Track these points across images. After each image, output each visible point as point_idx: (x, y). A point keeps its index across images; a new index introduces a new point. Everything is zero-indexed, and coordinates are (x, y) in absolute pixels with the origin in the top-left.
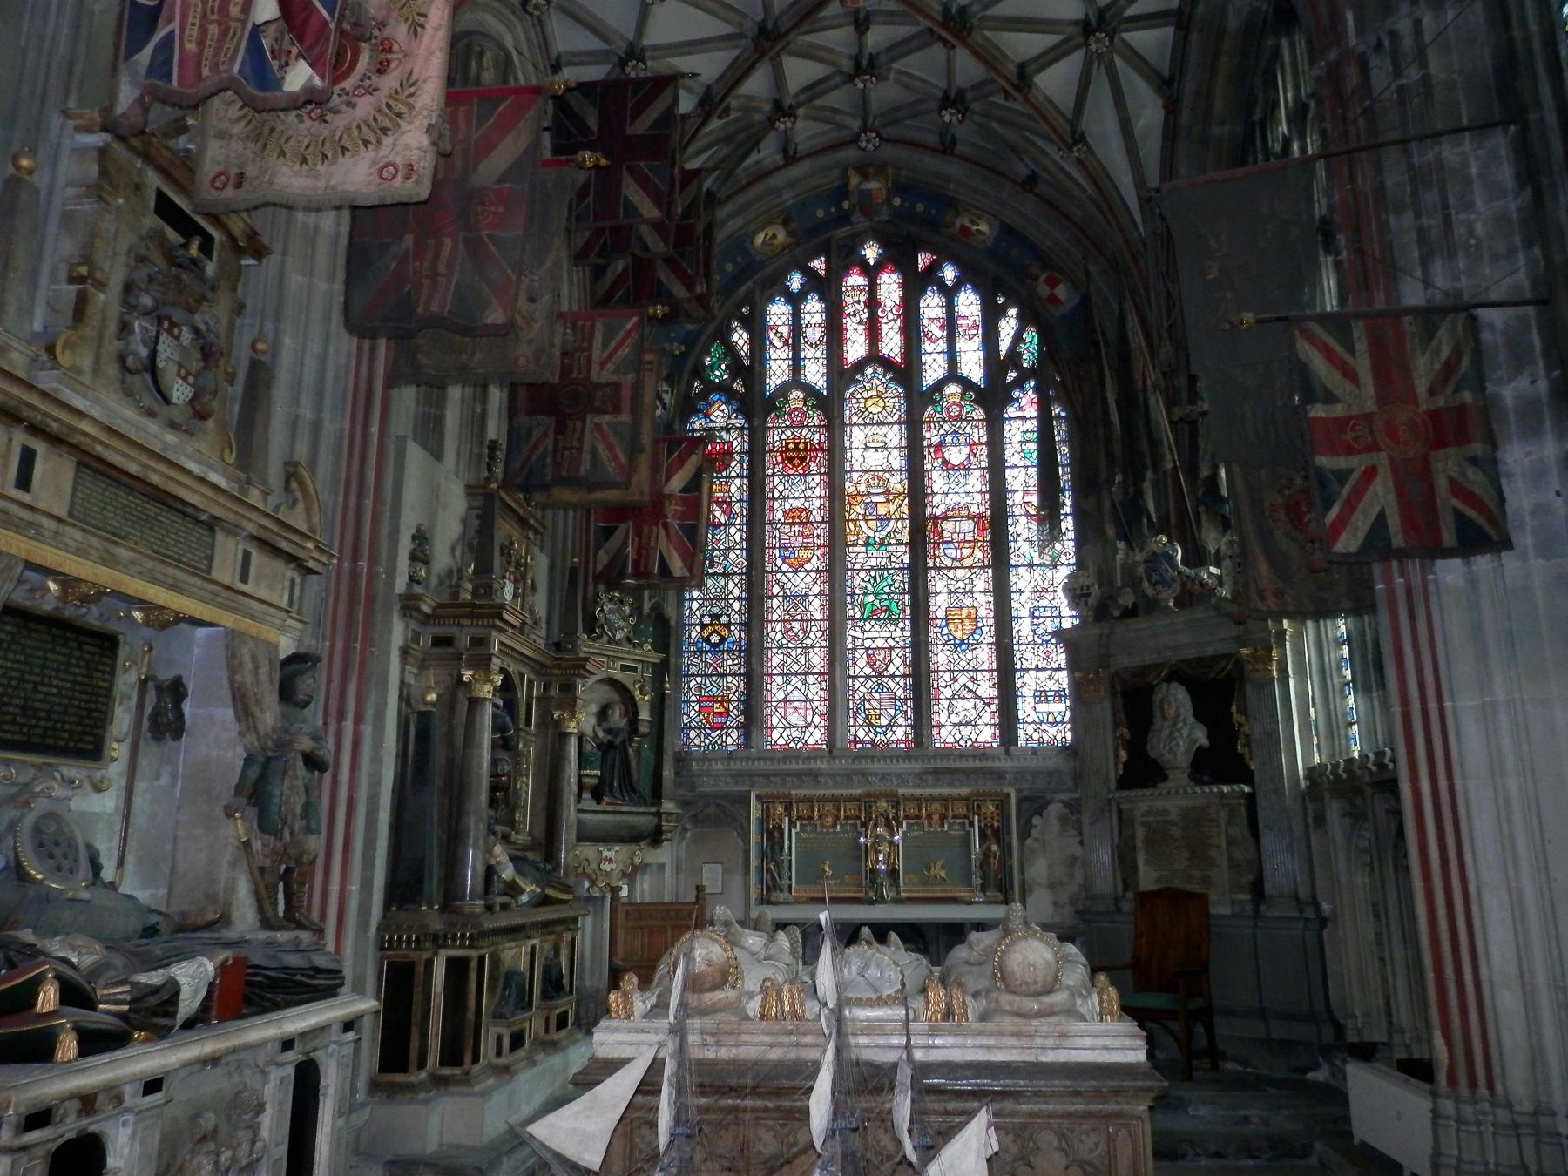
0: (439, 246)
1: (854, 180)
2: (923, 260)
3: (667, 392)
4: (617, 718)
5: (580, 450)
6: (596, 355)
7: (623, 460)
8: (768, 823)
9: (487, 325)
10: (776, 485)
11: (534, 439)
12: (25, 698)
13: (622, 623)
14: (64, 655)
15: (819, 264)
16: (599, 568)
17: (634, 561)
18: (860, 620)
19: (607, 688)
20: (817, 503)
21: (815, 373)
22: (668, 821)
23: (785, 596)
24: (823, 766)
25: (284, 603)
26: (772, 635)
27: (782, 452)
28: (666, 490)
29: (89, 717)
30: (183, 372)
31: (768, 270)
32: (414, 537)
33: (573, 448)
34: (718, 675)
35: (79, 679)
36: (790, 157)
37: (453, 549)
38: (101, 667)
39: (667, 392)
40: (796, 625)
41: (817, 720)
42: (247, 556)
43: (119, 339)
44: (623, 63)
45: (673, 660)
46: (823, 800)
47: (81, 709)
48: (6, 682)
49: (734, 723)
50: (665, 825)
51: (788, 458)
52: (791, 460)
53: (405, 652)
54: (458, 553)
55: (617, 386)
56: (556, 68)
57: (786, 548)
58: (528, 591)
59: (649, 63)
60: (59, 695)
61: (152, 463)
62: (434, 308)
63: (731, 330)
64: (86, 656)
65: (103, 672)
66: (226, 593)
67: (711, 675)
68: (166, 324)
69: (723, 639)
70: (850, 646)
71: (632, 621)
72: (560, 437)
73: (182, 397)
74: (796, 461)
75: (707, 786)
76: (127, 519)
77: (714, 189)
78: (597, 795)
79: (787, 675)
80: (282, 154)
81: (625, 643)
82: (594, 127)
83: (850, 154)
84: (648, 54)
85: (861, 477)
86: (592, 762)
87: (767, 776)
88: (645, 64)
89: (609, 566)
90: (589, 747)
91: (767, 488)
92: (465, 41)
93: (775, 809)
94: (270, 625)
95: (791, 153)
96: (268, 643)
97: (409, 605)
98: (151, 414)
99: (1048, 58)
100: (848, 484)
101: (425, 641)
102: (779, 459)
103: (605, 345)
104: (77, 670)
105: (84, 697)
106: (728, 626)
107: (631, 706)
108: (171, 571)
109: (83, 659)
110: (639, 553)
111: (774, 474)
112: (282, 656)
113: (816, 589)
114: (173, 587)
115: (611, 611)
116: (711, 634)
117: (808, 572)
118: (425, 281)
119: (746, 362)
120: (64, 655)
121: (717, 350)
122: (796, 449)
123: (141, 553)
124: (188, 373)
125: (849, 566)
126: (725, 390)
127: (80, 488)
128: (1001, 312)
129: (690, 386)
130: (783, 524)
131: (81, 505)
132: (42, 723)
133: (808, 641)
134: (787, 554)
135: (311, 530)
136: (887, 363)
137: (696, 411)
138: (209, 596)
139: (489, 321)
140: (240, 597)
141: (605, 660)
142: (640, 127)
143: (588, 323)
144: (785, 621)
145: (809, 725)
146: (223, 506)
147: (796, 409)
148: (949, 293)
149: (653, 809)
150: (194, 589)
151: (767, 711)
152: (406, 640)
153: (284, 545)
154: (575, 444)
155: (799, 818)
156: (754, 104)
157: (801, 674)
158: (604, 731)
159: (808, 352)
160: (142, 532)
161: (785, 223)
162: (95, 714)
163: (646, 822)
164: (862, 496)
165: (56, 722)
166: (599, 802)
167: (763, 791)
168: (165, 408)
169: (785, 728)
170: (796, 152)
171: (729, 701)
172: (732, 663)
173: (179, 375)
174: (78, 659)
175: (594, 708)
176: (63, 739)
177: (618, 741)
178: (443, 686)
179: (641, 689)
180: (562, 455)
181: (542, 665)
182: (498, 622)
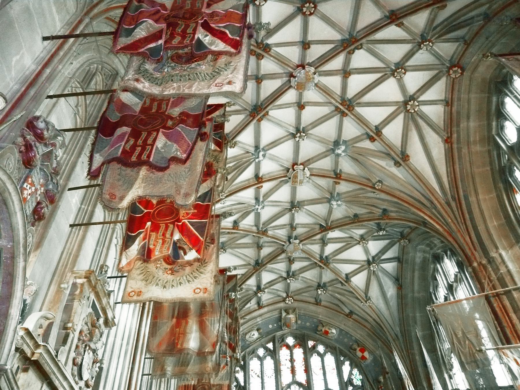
1: (284, 314)
2: (311, 343)
36: (260, 306)
83: (282, 305)
99: (356, 272)
128: (343, 363)
136: (300, 385)
148: (322, 356)
156: (250, 287)
161: (258, 330)
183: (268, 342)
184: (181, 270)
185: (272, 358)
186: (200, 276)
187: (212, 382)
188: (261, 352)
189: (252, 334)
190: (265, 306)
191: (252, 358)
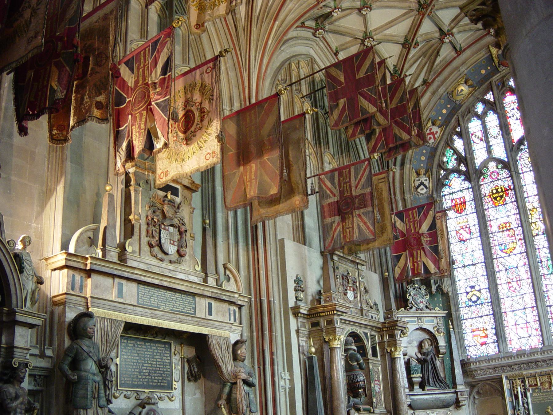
0: (251, 167)
3: (426, 180)
4: (427, 346)
6: (353, 184)
7: (372, 228)
8: (514, 390)
9: (272, 195)
10: (491, 213)
11: (334, 228)
12: (140, 369)
13: (422, 300)
14: (151, 352)
15: (490, 96)
16: (397, 276)
17: (412, 269)
18: (548, 275)
19: (418, 332)
20: (514, 217)
21: (500, 152)
22: (461, 395)
23: (506, 270)
24: (539, 356)
25: (232, 321)
26: (503, 291)
27: (490, 196)
28: (420, 232)
29: (164, 374)
30: (172, 242)
31: (463, 108)
32: (295, 281)
33: (350, 228)
34: (479, 317)
35: (158, 360)
36: (459, 52)
37: (318, 282)
38: (165, 355)
39: (426, 180)
40: (514, 284)
41: (534, 333)
42: (210, 305)
43: (147, 237)
44: (363, 42)
45: (454, 313)
46: (541, 375)
47: (161, 371)
48: (132, 364)
49: (492, 341)
50: (461, 398)
51: (494, 198)
52: (495, 198)
53: (298, 331)
54: (321, 283)
55: (363, 195)
56: (336, 54)
57: (502, 245)
58: (363, 293)
59: (375, 37)
60: (152, 367)
61: (163, 278)
62: (252, 194)
63: (452, 141)
64: (159, 351)
65: (167, 357)
66: (202, 321)
67: (475, 318)
68: (163, 226)
69: (478, 298)
70: (545, 290)
71: (428, 297)
72: (344, 224)
73: (173, 251)
74: (498, 198)
75: (480, 376)
76: (159, 300)
77: (426, 78)
78: (422, 386)
79: (514, 311)
80: (176, 160)
81: (425, 308)
82: (343, 80)
84: (373, 33)
85: (534, 199)
86: (417, 371)
87: (510, 366)
88: (372, 38)
89: (401, 274)
90: (414, 363)
91: (486, 216)
92: (288, 62)
93: (516, 383)
94: (225, 330)
95: (458, 49)
96: (224, 338)
97: (296, 312)
98: (162, 260)
100: (527, 204)
101: (308, 325)
102: (490, 199)
103: (356, 178)
104: (157, 357)
105: (161, 366)
106: (479, 291)
107: (434, 340)
108: (178, 316)
109: (158, 353)
110: (414, 265)
111: (488, 208)
112: (233, 341)
113: (521, 263)
114: (180, 322)
115: (414, 295)
116: (472, 296)
117: (515, 255)
118: (249, 183)
119: (463, 154)
120: (151, 352)
121: (449, 152)
122: (497, 192)
123: (165, 312)
124: (174, 241)
125: (537, 247)
126: (456, 171)
127: (140, 293)
129: (438, 173)
130: (498, 232)
131: (142, 299)
132: (147, 377)
133: (522, 292)
134: (503, 247)
135: (238, 290)
137: (444, 185)
138: (197, 323)
139: (272, 193)
140: (209, 321)
141: (416, 319)
142: (361, 74)
143: (348, 170)
144: (509, 283)
145: (530, 336)
146: (195, 288)
147: (493, 172)
149: (453, 390)
150: (188, 321)
151: (507, 332)
152: (298, 327)
153: (224, 298)
154: (351, 226)
155: (530, 386)
156: (430, 36)
157: (521, 309)
158: (421, 354)
159: (492, 142)
160: (166, 304)
161: (466, 82)
162: (165, 372)
163: (449, 397)
164: (536, 208)
165: (152, 376)
166: (423, 390)
167: (508, 374)
168: (168, 256)
169: (519, 339)
170: (461, 47)
171: (487, 329)
172: (487, 309)
173: (170, 243)
174: (156, 353)
175: (416, 344)
176: (156, 382)
177: (429, 357)
178: (318, 345)
179: (438, 330)
180: (346, 231)
181: (380, 328)
183: (486, 92)
184: (192, 137)
185: (495, 112)
186: (209, 138)
188: (480, 108)
189: (460, 90)
191: (469, 120)
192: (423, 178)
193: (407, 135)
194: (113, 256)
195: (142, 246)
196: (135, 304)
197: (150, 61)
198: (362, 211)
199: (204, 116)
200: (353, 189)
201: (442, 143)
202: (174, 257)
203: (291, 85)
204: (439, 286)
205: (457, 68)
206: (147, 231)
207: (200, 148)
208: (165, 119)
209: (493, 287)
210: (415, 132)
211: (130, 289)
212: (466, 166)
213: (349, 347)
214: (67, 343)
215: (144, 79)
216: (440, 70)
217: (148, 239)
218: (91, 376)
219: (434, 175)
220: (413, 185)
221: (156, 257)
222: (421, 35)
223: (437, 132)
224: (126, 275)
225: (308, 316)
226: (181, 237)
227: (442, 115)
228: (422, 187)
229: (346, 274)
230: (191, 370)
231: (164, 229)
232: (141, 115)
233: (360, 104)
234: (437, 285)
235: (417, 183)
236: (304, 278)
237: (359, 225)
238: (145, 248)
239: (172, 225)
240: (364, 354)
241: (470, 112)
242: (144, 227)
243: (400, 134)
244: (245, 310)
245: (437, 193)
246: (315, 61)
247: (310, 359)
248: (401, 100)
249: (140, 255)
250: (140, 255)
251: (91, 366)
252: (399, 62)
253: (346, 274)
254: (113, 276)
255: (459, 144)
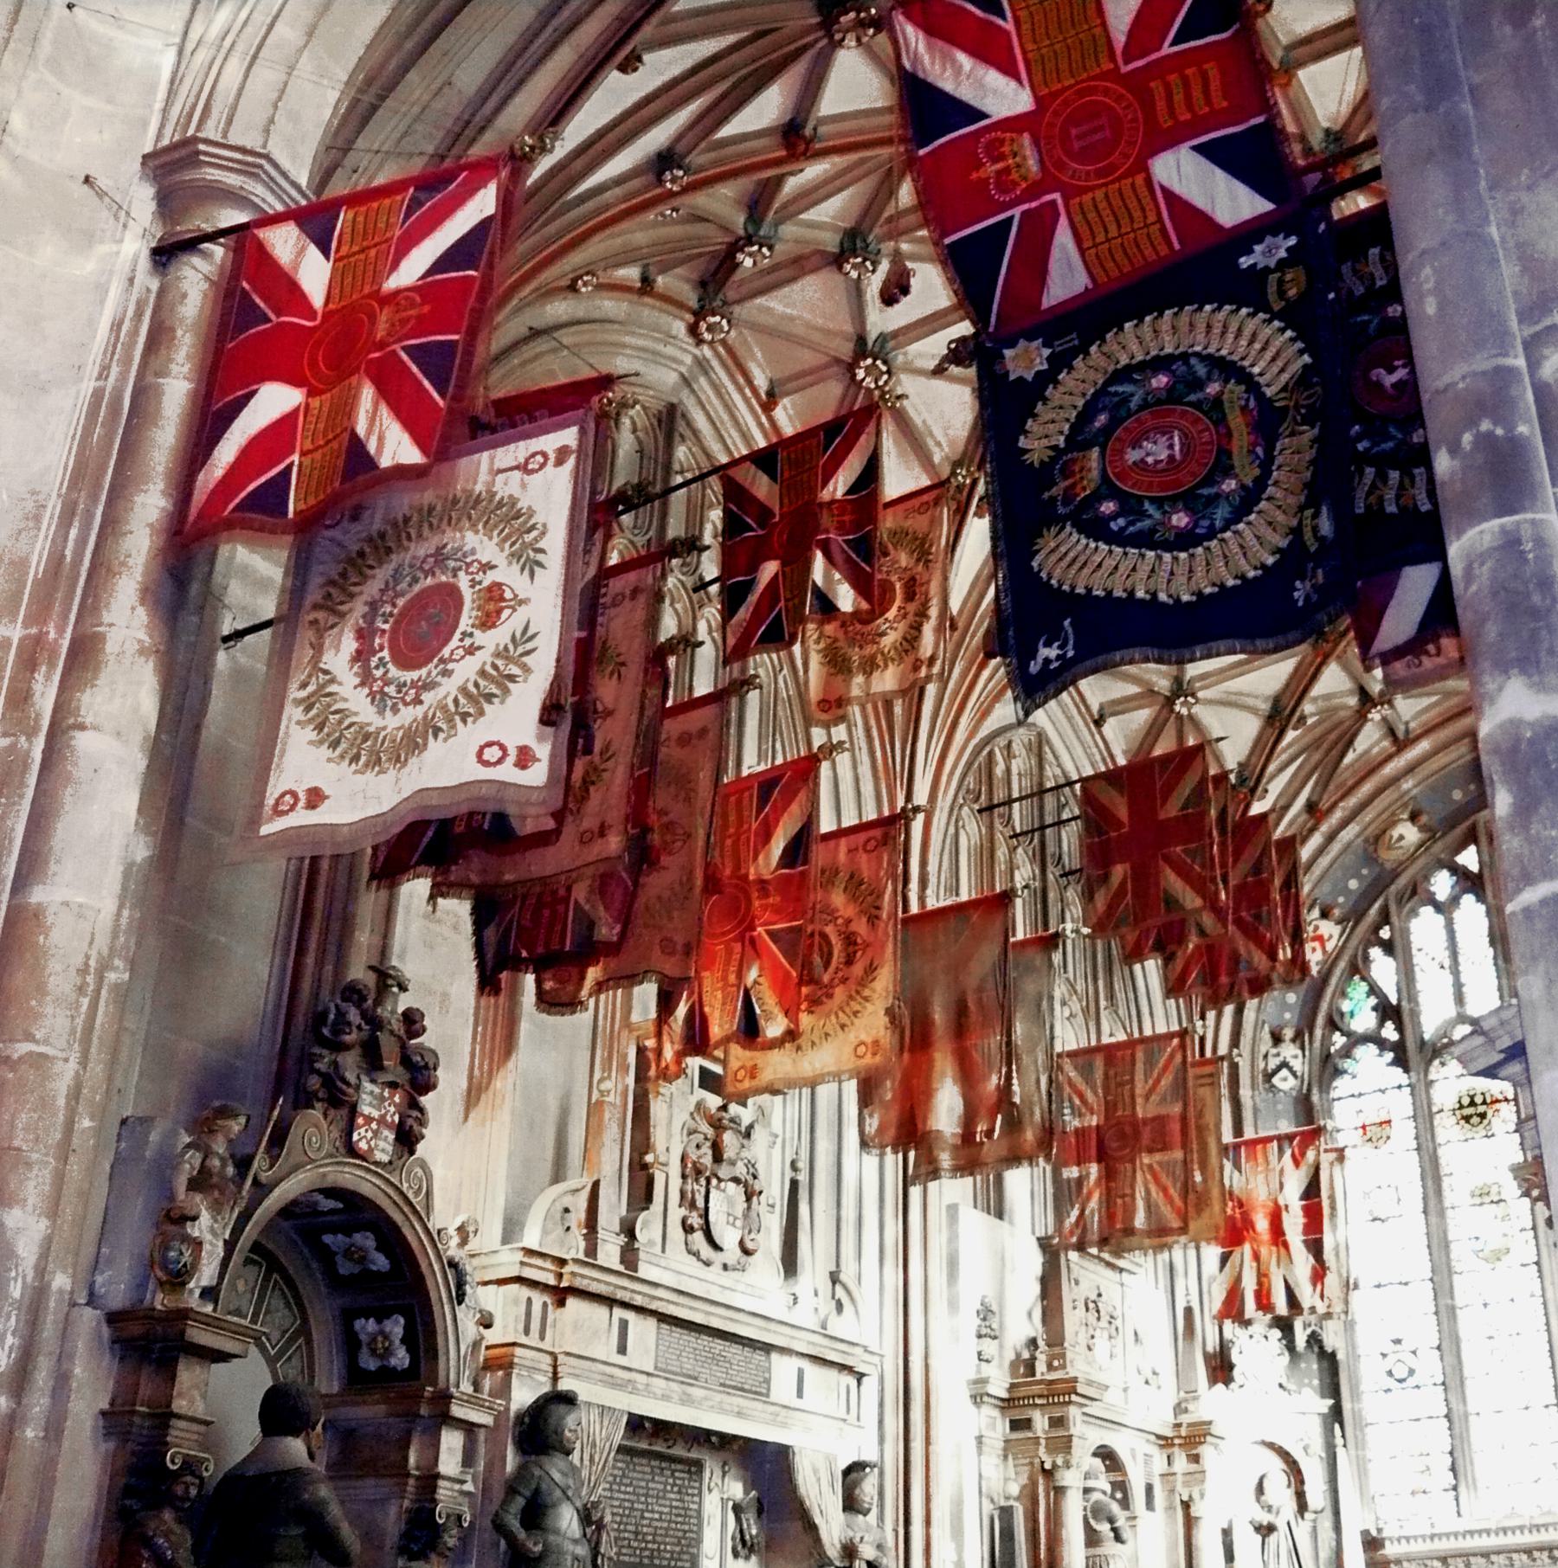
3: (1296, 1057)
5: (1133, 1196)
6: (1140, 1089)
15: (1469, 858)
31: (1402, 881)
36: (1400, 741)
39: (1296, 1057)
45: (1347, 1406)
63: (1366, 959)
68: (714, 1182)
69: (1411, 1372)
77: (1314, 798)
95: (1401, 734)
98: (707, 1264)
103: (1147, 1076)
114: (740, 1414)
121: (1359, 989)
122: (1472, 1104)
129: (1326, 1043)
137: (1338, 1072)
154: (1128, 1191)
161: (1413, 818)
170: (1407, 731)
181: (1166, 1438)
182: (1074, 1398)
185: (1481, 898)
187: (1140, 1113)
188: (1442, 884)
190: (1418, 738)
191: (1414, 913)
192: (1289, 1051)
193: (1264, 957)
194: (609, 1253)
195: (669, 1229)
196: (651, 1370)
197: (754, 826)
198: (1158, 1157)
199: (855, 953)
200: (1139, 1101)
201: (1342, 964)
202: (732, 1252)
203: (990, 808)
204: (1313, 1333)
205: (1395, 780)
206: (683, 1194)
207: (843, 1027)
208: (788, 974)
209: (1449, 1345)
210: (1285, 953)
211: (642, 1331)
212: (1400, 1028)
213: (1091, 1484)
214: (511, 1460)
215: (737, 867)
216: (1350, 783)
217: (683, 1212)
218: (569, 1547)
219: (1317, 1044)
220: (1262, 1065)
221: (696, 1254)
222: (1315, 700)
223: (1331, 937)
224: (638, 1300)
225: (1007, 1404)
226: (749, 1208)
227: (1346, 891)
228: (1284, 1072)
229: (1093, 1297)
230: (741, 1531)
231: (718, 1187)
232: (729, 952)
233: (1163, 883)
234: (1309, 1331)
235: (1273, 1063)
236: (1001, 1306)
237: (1148, 1192)
238: (676, 1232)
239: (736, 1180)
240: (1125, 1503)
241: (1417, 893)
242: (676, 1183)
243: (1249, 952)
244: (870, 1384)
245: (1321, 1092)
246: (1048, 742)
247: (1006, 1513)
248: (1257, 868)
249: (663, 1251)
250: (663, 1251)
251: (567, 1520)
252: (1254, 760)
253: (1093, 1297)
254: (610, 1302)
255: (1383, 968)
